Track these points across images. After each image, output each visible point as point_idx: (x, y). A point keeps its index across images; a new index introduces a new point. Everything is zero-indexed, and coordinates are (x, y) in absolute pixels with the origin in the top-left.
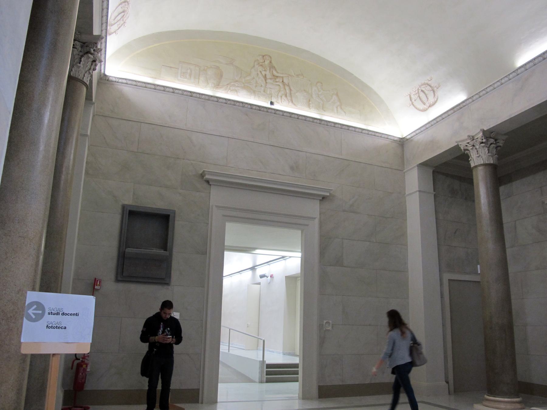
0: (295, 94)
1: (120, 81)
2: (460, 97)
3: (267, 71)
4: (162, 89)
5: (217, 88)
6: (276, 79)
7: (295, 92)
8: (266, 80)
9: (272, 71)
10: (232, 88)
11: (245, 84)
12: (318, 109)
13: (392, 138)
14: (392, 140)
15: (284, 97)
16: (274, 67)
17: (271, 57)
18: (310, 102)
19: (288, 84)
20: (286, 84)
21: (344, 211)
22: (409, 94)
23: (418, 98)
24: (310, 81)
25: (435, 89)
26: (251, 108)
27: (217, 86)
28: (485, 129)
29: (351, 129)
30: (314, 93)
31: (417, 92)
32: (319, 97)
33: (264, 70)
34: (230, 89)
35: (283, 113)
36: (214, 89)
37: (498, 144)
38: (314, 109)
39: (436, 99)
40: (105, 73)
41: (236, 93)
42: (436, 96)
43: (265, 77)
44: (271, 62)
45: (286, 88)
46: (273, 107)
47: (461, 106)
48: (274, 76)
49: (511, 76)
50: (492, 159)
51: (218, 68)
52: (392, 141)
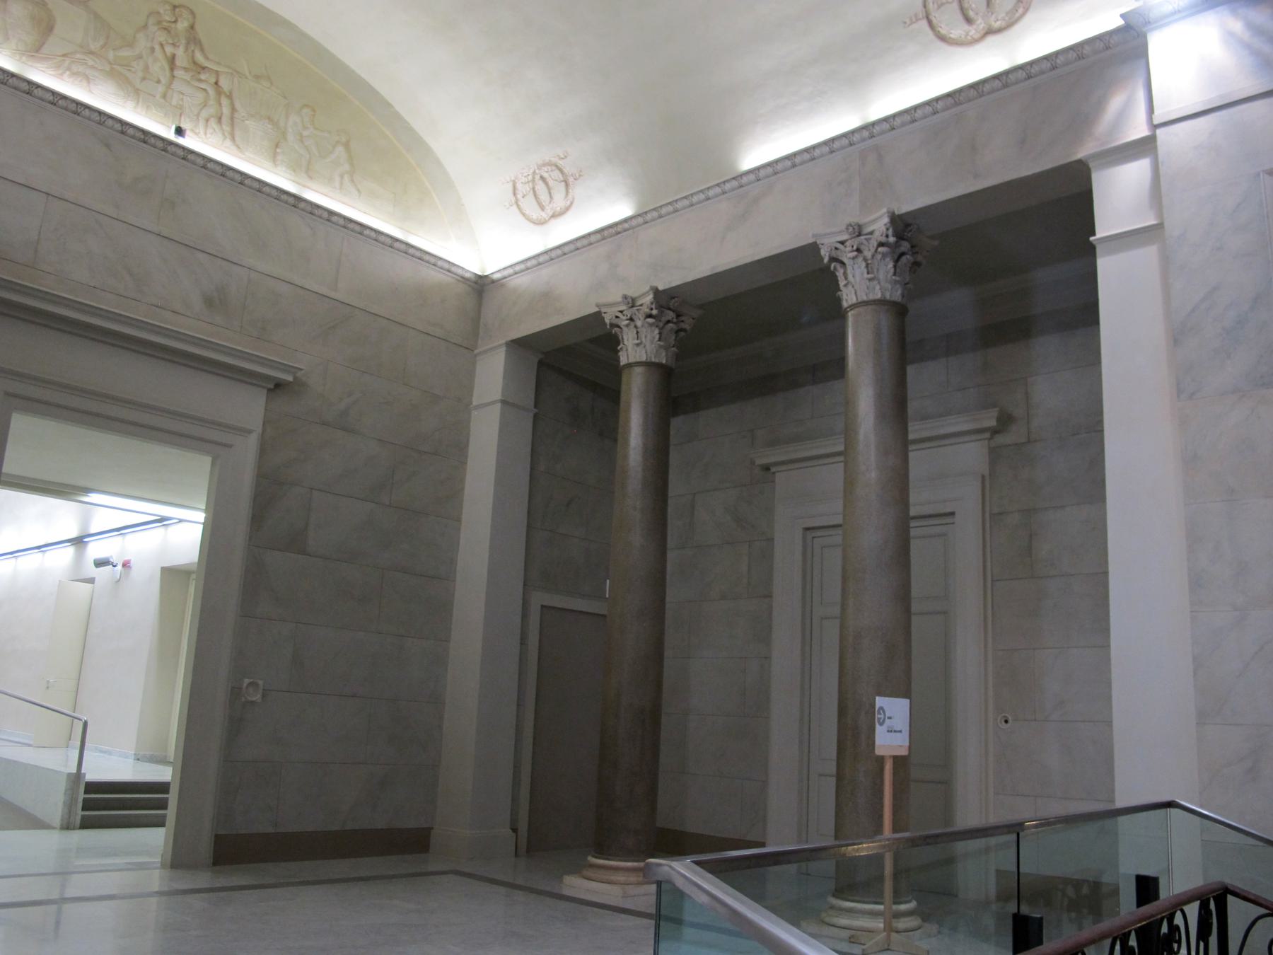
0: (243, 121)
2: (619, 209)
3: (178, 46)
5: (32, 56)
6: (199, 73)
7: (243, 117)
8: (172, 69)
9: (193, 51)
10: (75, 68)
11: (115, 66)
12: (294, 171)
13: (460, 272)
15: (213, 123)
16: (200, 42)
17: (192, 13)
19: (231, 93)
20: (225, 93)
22: (513, 178)
23: (532, 192)
24: (285, 98)
25: (571, 180)
26: (123, 133)
27: (35, 51)
28: (661, 288)
29: (367, 232)
30: (290, 130)
31: (530, 177)
32: (302, 142)
33: (171, 42)
34: (69, 69)
36: (24, 58)
37: (682, 325)
38: (284, 169)
39: (568, 203)
41: (85, 83)
42: (570, 196)
43: (172, 60)
44: (192, 27)
45: (222, 102)
46: (180, 141)
47: (619, 228)
48: (195, 63)
49: (728, 186)
50: (664, 354)
52: (459, 278)
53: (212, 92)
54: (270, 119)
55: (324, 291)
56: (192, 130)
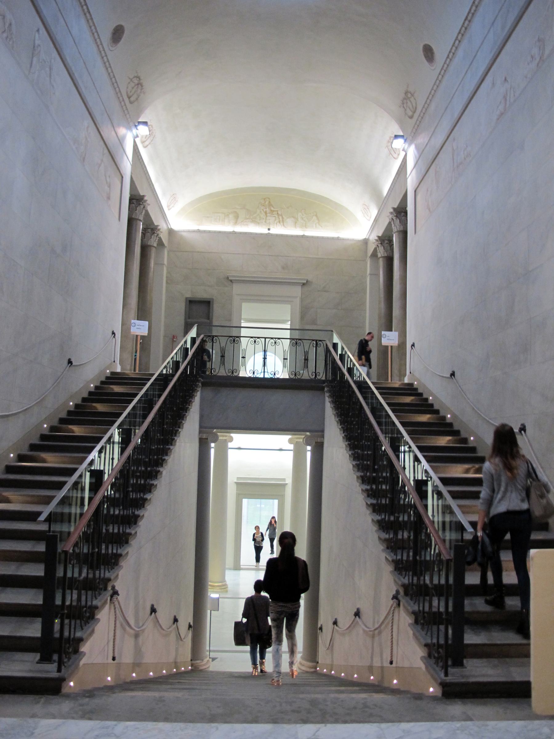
8: (266, 215)
15: (278, 224)
16: (272, 205)
17: (269, 198)
19: (281, 214)
21: (319, 291)
24: (296, 209)
27: (236, 223)
30: (299, 217)
35: (277, 235)
40: (172, 228)
43: (266, 213)
44: (269, 202)
48: (271, 210)
51: (236, 212)
53: (277, 216)
55: (315, 256)
56: (273, 228)
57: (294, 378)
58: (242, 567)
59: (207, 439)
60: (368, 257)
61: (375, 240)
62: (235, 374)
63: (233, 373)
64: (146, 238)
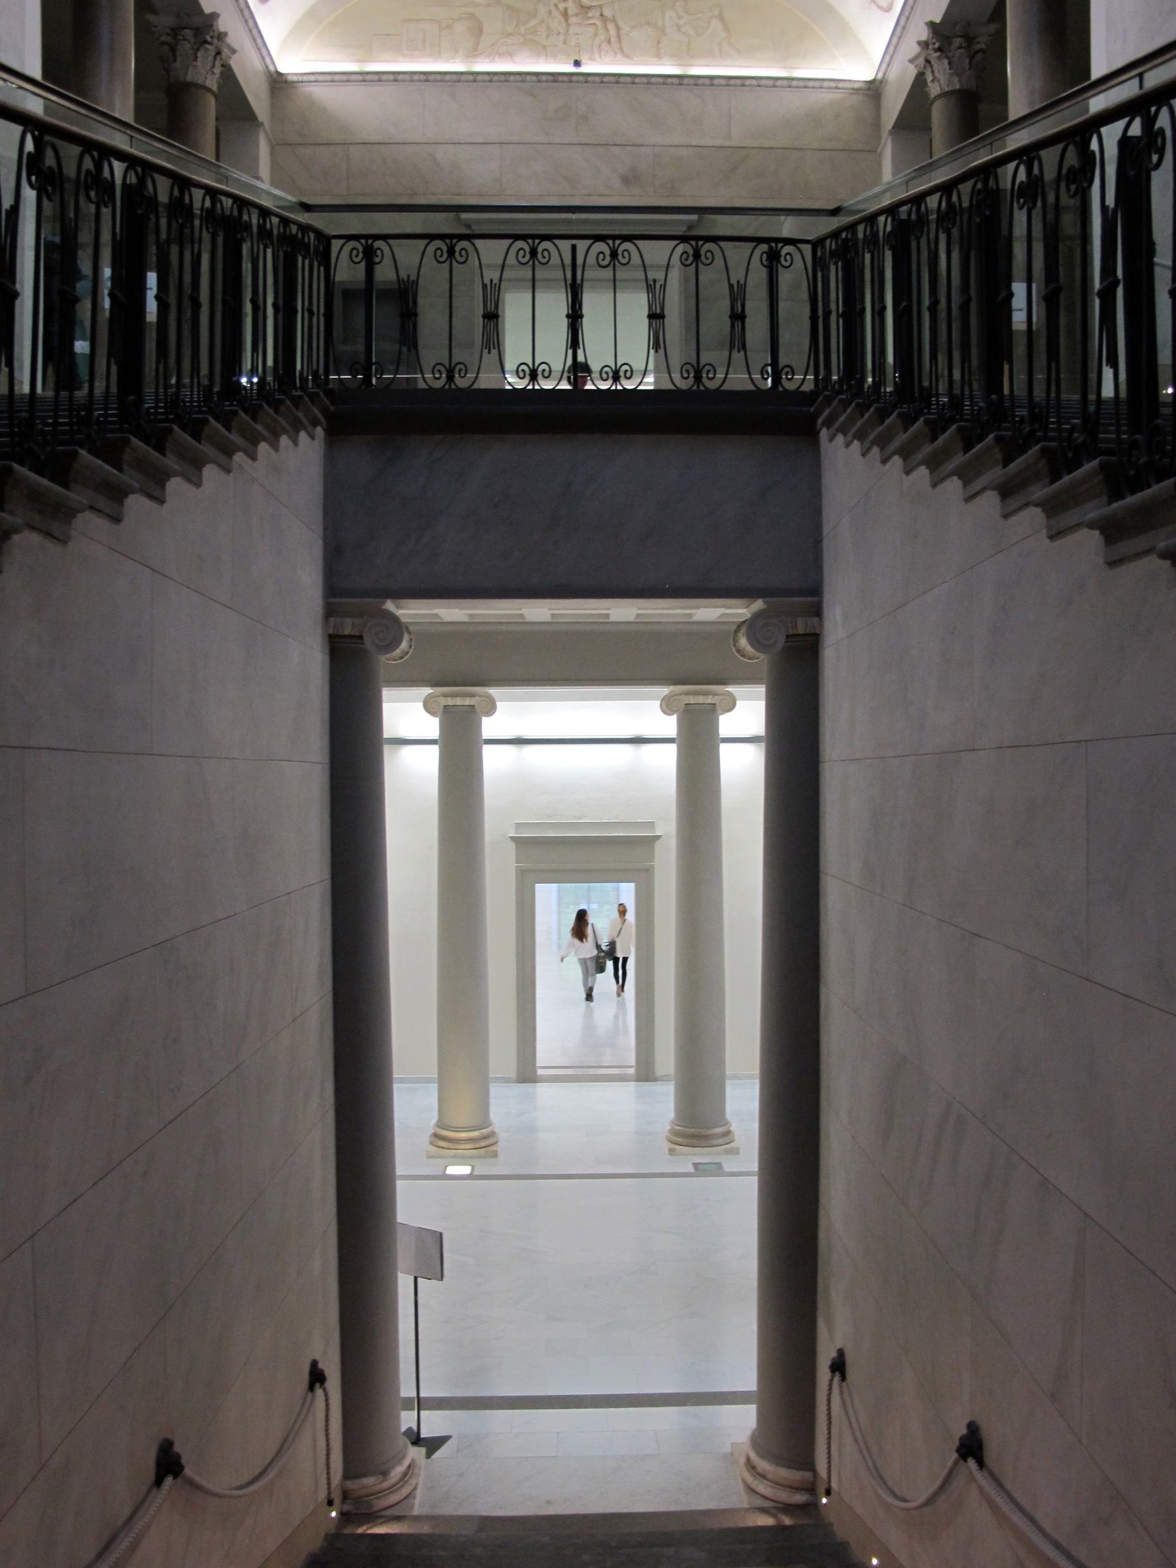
1: (305, 78)
4: (376, 77)
5: (474, 55)
6: (587, 13)
7: (627, 31)
8: (566, 20)
13: (848, 85)
14: (848, 89)
15: (605, 46)
18: (660, 46)
19: (614, 17)
20: (610, 19)
26: (540, 81)
27: (474, 53)
29: (748, 82)
32: (679, 29)
35: (602, 79)
36: (469, 59)
37: (978, 47)
43: (565, 14)
45: (608, 27)
48: (582, 7)
50: (956, 80)
51: (473, 16)
52: (852, 91)
53: (599, 23)
54: (648, 23)
55: (719, 142)
57: (695, 388)
58: (540, 1072)
59: (361, 637)
60: (885, 134)
61: (919, 43)
62: (461, 382)
63: (450, 378)
64: (179, 59)
